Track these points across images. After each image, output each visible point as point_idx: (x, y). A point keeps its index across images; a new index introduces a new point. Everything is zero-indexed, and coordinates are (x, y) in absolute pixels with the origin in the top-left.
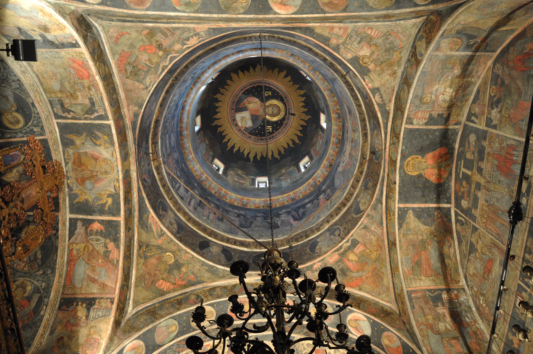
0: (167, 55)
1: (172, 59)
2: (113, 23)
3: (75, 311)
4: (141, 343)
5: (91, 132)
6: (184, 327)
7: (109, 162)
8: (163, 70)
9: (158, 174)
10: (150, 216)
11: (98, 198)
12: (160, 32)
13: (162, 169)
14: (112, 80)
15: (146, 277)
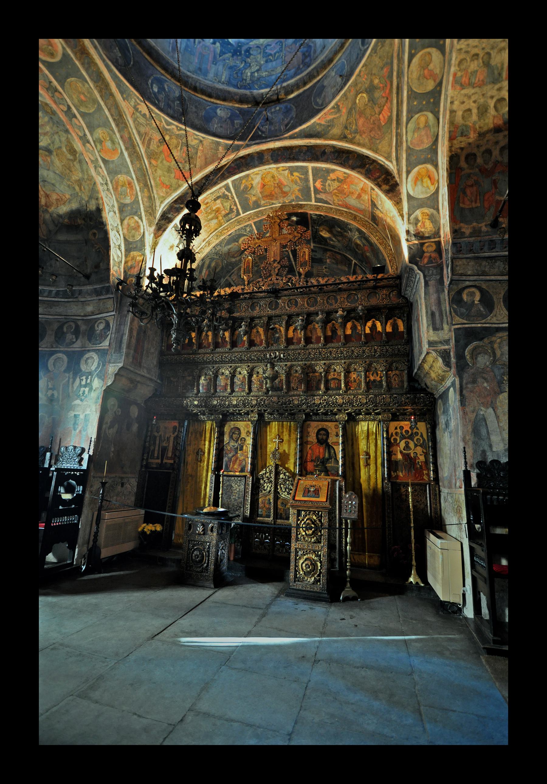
0: (167, 130)
1: (169, 124)
2: (156, 196)
3: (378, 216)
4: (416, 170)
5: (243, 193)
6: (428, 102)
7: (264, 176)
8: (181, 129)
9: (292, 92)
10: (318, 122)
11: (296, 183)
12: (149, 148)
13: (288, 85)
14: (200, 180)
15: (372, 136)
